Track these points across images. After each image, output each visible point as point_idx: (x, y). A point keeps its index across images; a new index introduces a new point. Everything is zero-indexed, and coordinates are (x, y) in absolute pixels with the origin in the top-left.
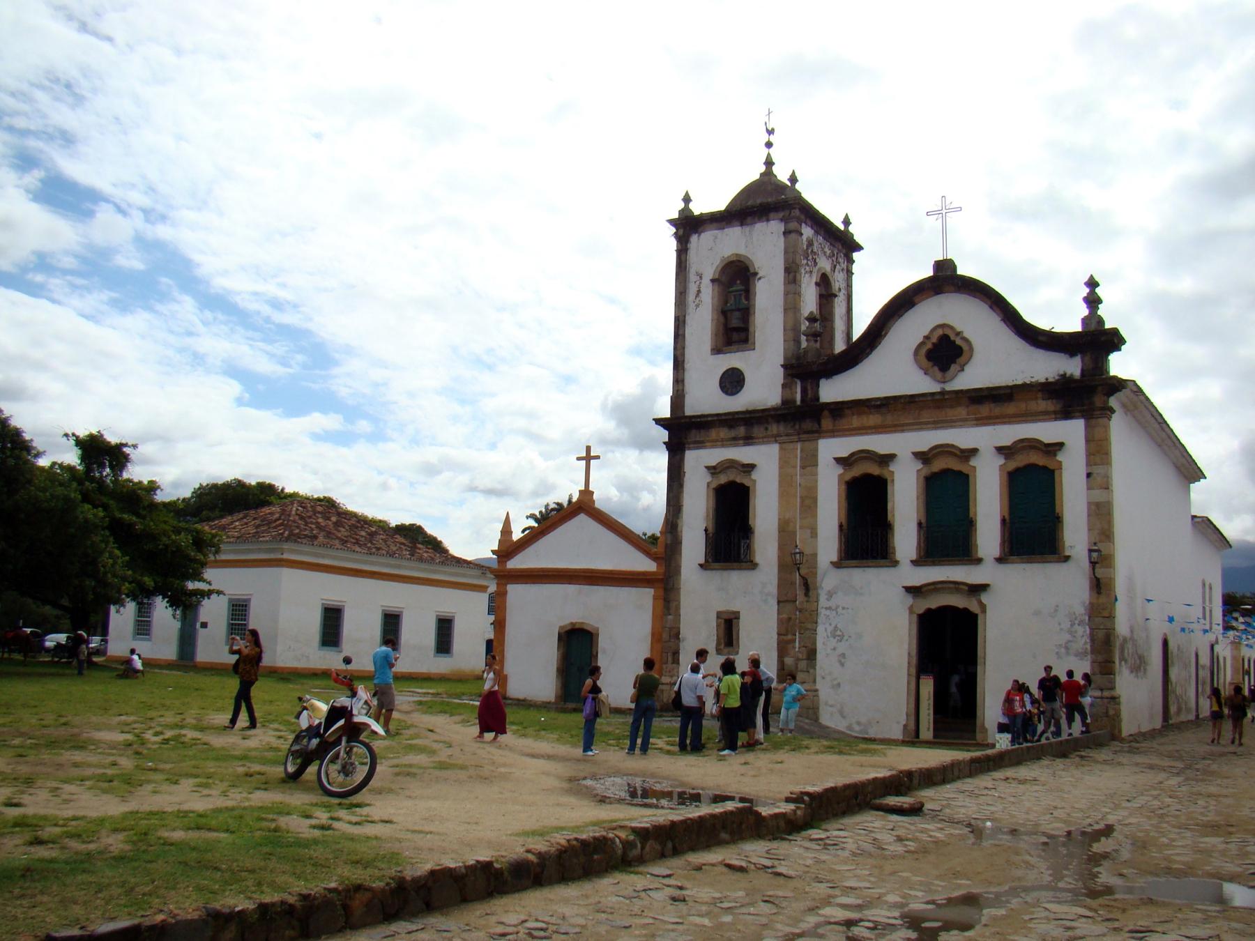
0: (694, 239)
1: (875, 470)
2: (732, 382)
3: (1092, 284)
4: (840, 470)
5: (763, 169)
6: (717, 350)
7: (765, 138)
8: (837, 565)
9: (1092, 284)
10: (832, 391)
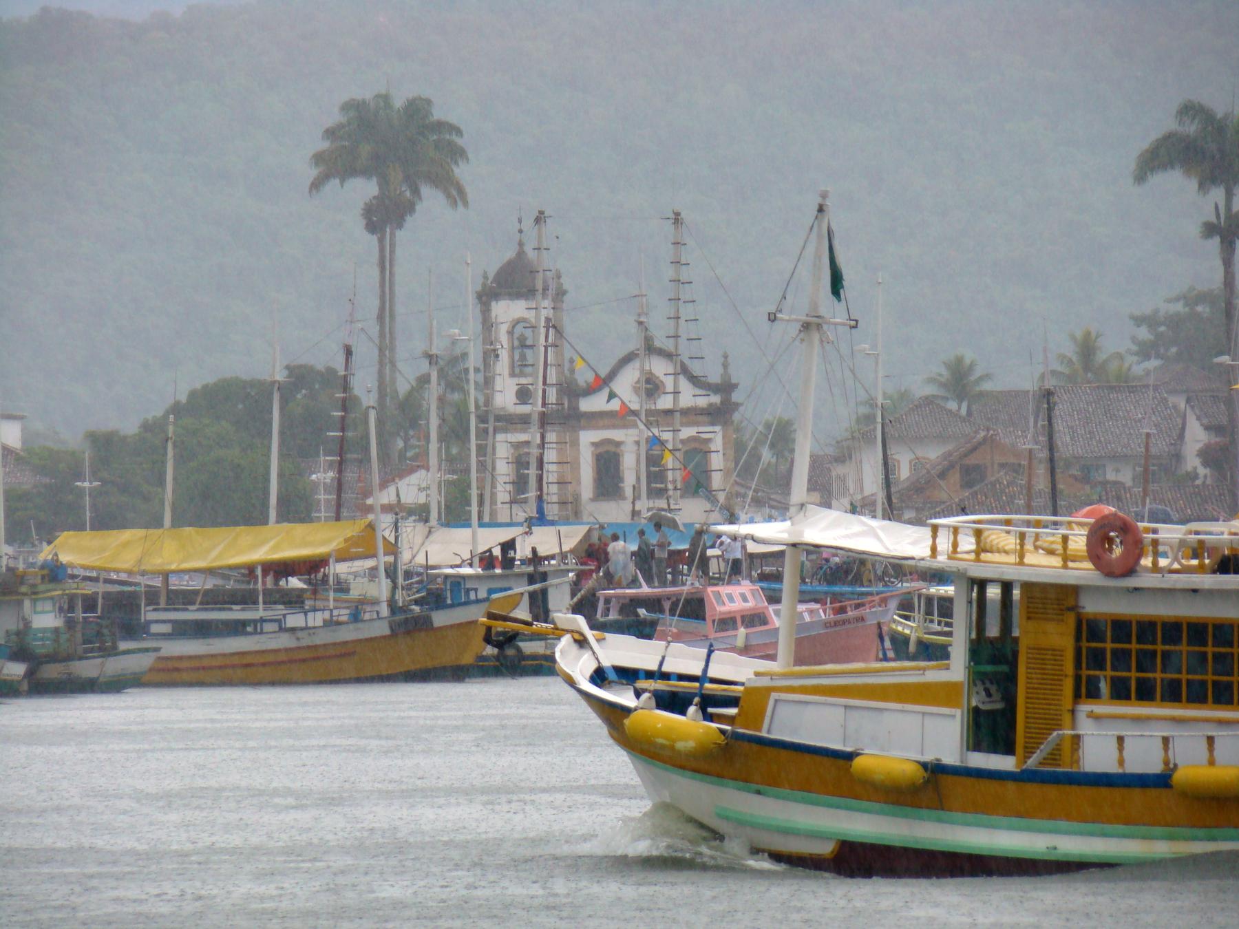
0: (493, 304)
1: (613, 449)
2: (523, 395)
3: (726, 357)
4: (593, 449)
5: (517, 247)
6: (513, 375)
7: (517, 226)
8: (593, 500)
9: (726, 357)
10: (588, 405)
